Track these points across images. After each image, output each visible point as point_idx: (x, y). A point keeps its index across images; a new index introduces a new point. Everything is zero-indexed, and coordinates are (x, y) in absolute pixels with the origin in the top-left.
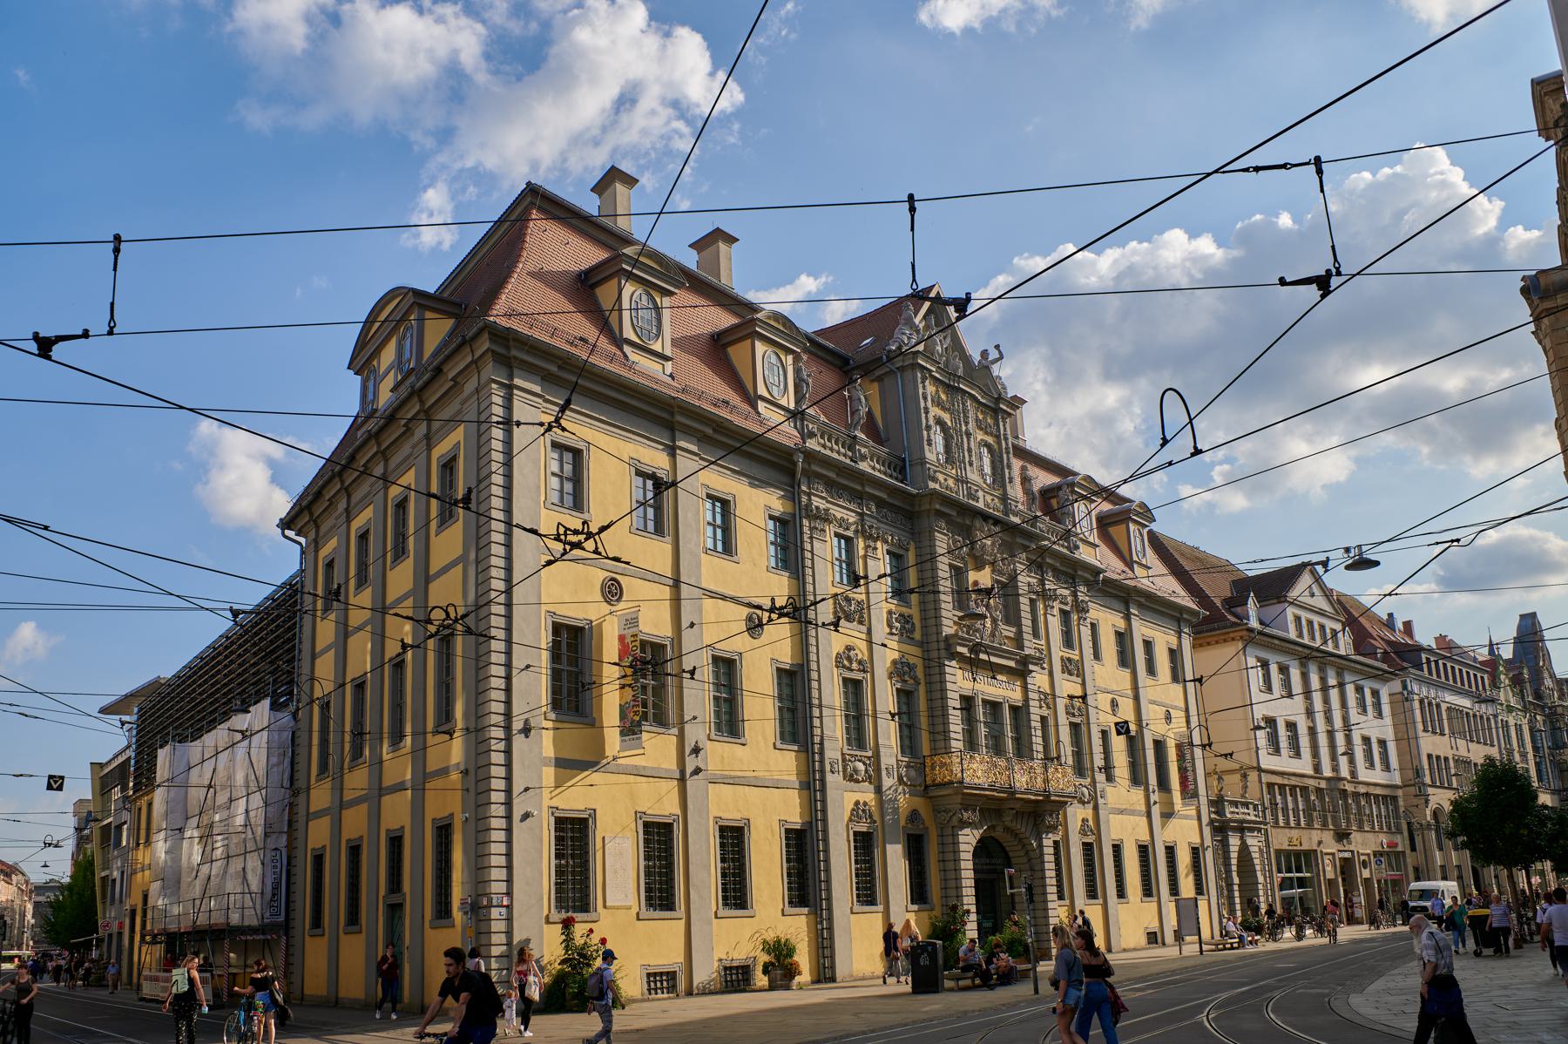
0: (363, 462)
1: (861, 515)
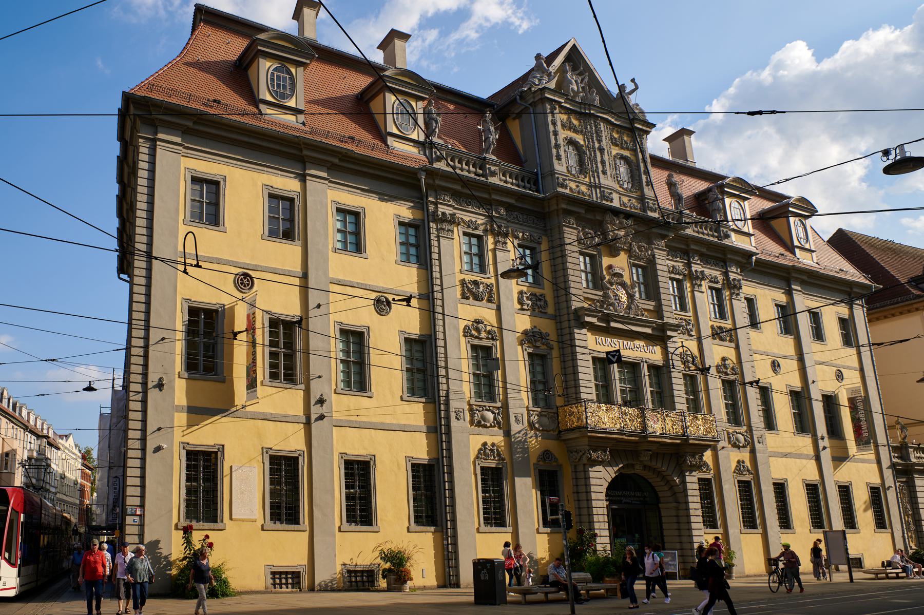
1: (491, 218)
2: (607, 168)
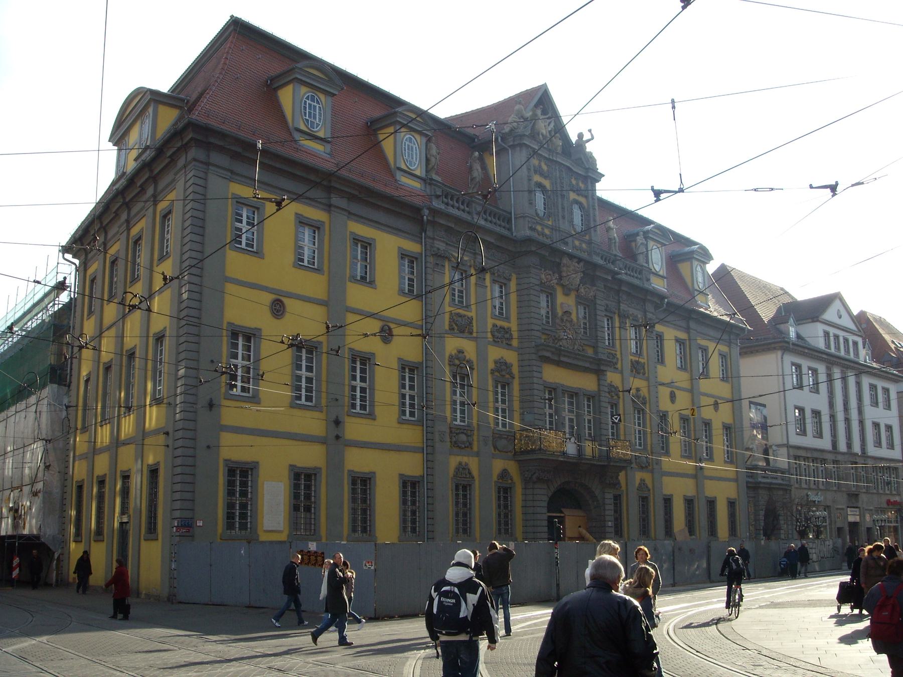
0: (114, 210)
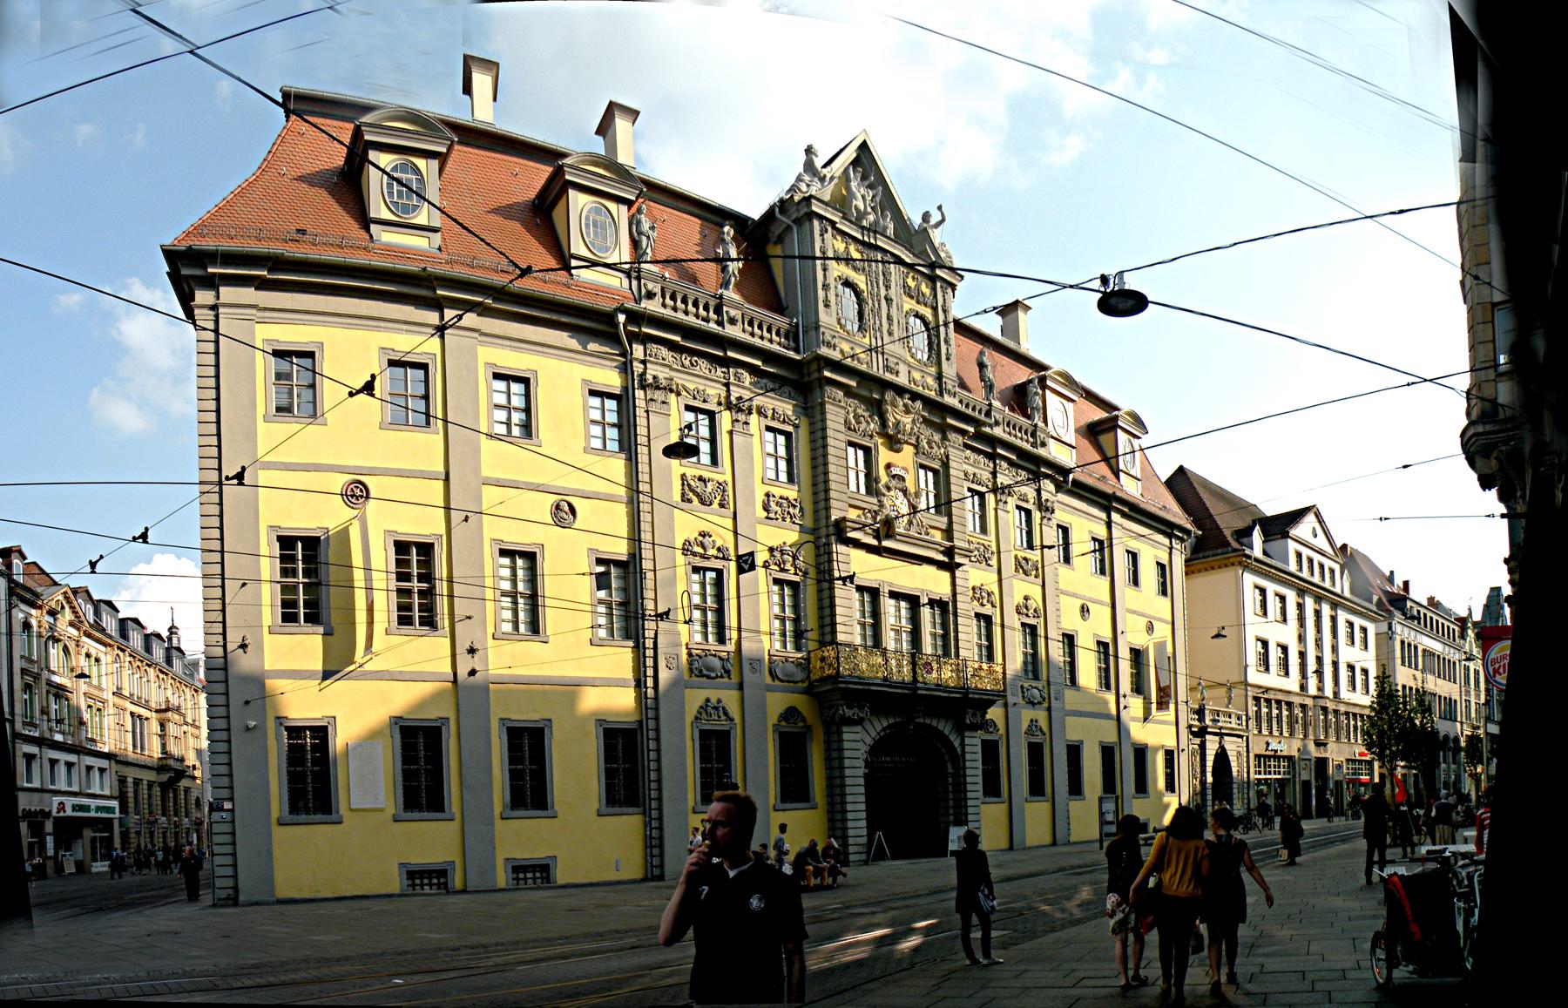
2: (895, 327)
